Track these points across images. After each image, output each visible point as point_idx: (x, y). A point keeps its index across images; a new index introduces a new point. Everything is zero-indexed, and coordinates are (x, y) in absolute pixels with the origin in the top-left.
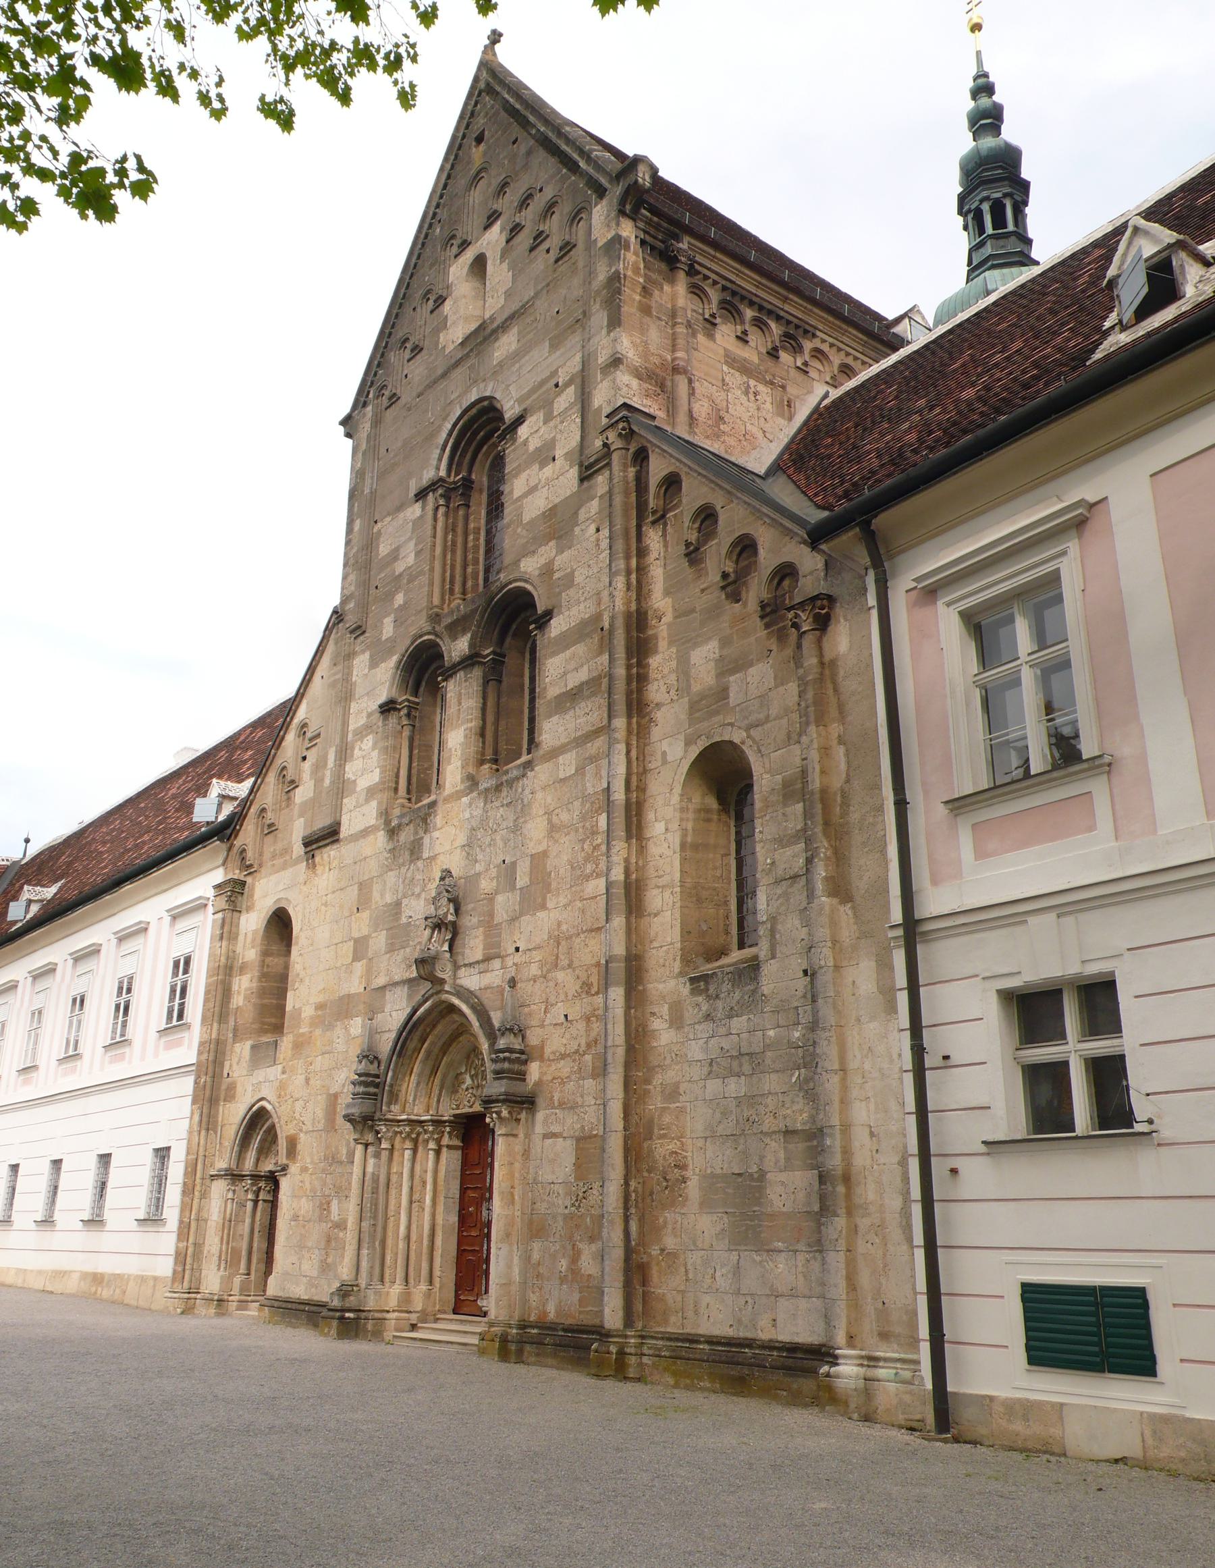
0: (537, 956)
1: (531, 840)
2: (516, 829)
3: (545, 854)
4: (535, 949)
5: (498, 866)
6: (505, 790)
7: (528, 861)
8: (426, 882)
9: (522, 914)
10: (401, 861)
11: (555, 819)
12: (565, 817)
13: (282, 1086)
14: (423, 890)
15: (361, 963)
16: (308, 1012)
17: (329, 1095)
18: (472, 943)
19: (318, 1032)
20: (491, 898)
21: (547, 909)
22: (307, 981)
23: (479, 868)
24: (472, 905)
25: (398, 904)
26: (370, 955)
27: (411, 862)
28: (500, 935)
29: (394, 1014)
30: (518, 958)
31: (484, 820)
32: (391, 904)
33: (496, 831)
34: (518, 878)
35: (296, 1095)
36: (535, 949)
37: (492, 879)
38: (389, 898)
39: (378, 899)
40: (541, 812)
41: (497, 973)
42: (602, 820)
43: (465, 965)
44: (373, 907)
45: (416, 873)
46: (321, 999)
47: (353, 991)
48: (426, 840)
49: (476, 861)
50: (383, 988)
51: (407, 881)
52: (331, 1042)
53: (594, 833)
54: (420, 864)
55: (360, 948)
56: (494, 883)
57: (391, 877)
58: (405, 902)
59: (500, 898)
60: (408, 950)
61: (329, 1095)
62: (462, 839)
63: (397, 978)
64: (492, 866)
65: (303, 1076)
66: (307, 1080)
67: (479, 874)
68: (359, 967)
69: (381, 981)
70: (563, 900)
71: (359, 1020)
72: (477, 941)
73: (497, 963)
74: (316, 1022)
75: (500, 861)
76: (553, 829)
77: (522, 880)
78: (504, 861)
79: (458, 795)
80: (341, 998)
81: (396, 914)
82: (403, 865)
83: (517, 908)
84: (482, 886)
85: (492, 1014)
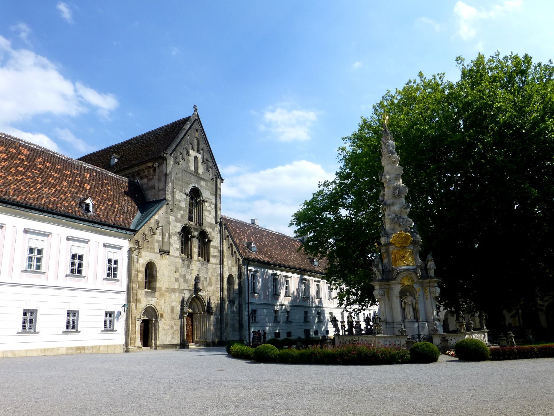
0: (210, 293)
2: (207, 272)
6: (205, 265)
12: (214, 274)
13: (157, 302)
16: (163, 288)
17: (171, 307)
19: (167, 293)
20: (203, 281)
22: (163, 282)
25: (185, 275)
31: (201, 268)
35: (162, 305)
38: (183, 273)
42: (219, 277)
46: (167, 287)
47: (176, 288)
48: (191, 266)
50: (183, 289)
52: (171, 296)
53: (218, 278)
55: (177, 280)
57: (183, 269)
59: (205, 282)
61: (171, 307)
62: (197, 269)
63: (186, 288)
65: (163, 302)
66: (165, 303)
68: (177, 284)
69: (182, 288)
70: (214, 286)
71: (178, 294)
73: (205, 292)
74: (165, 291)
76: (212, 275)
77: (208, 281)
79: (197, 261)
80: (173, 288)
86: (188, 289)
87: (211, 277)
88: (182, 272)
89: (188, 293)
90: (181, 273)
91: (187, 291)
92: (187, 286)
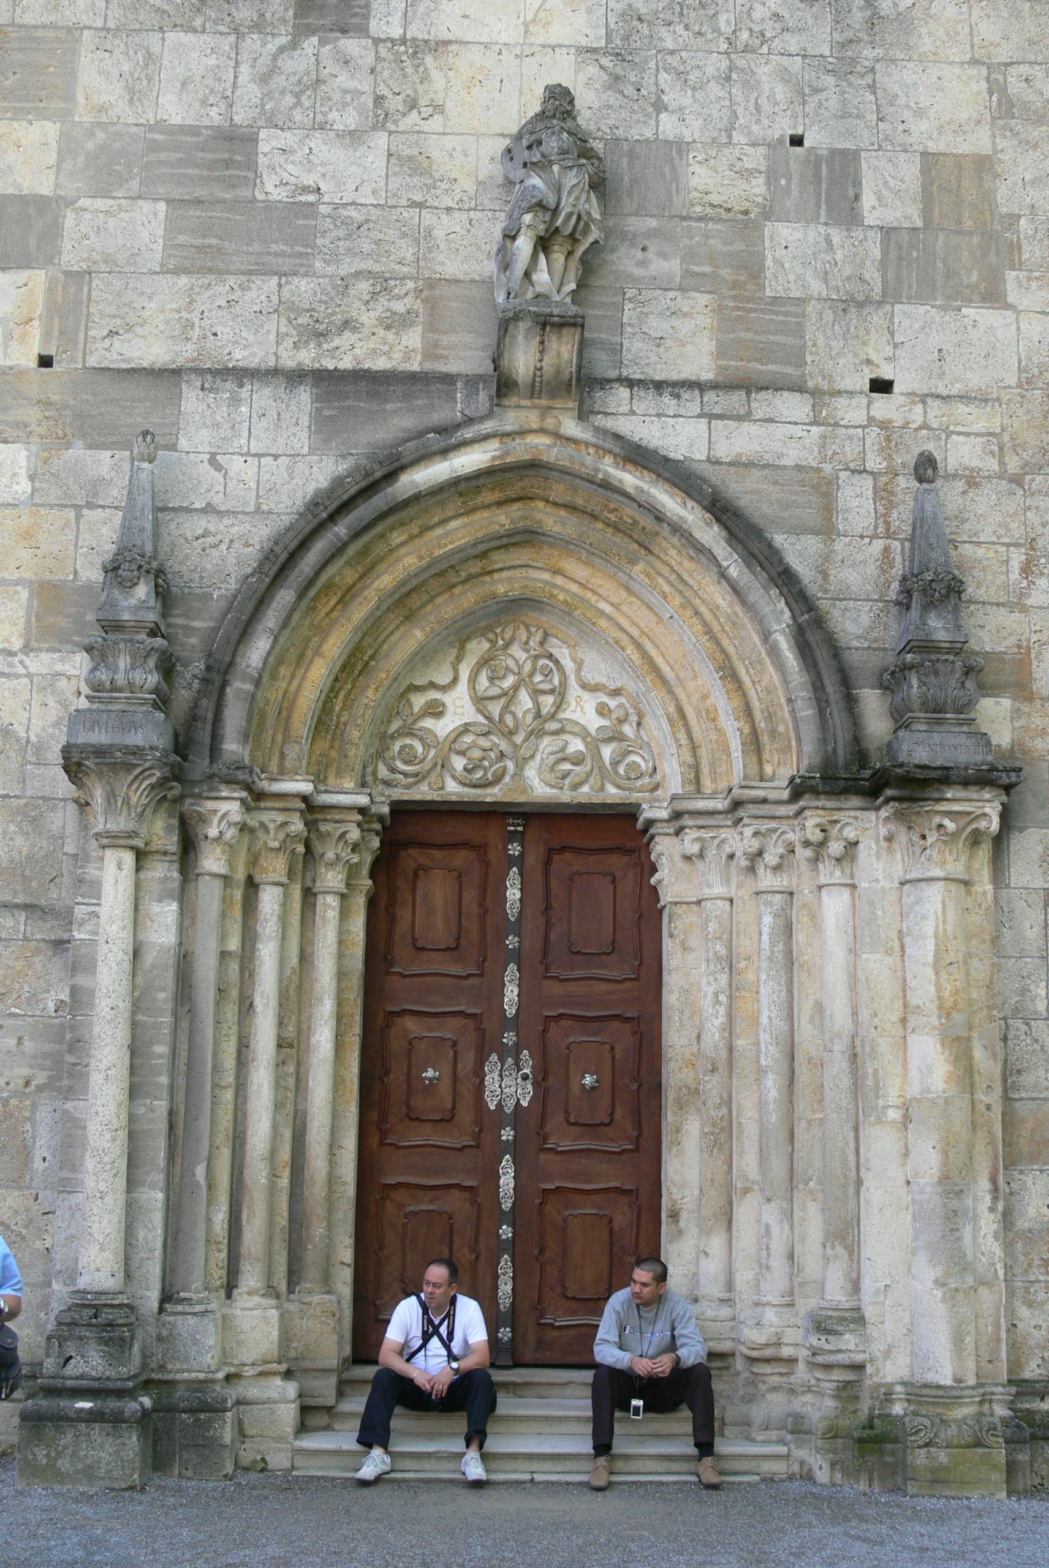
1: (920, 113)
3: (984, 165)
4: (964, 398)
5: (773, 146)
7: (910, 170)
8: (395, 104)
9: (891, 295)
10: (245, 14)
11: (1015, 86)
14: (378, 126)
15: (22, 276)
18: (656, 325)
21: (1008, 307)
23: (668, 126)
24: (652, 223)
26: (71, 257)
27: (301, 32)
28: (799, 331)
29: (235, 465)
30: (882, 406)
32: (194, 131)
33: (747, 49)
34: (868, 200)
36: (964, 398)
37: (747, 174)
39: (112, 94)
40: (957, 53)
41: (798, 431)
43: (631, 383)
44: (83, 116)
45: (331, 67)
49: (660, 107)
51: (279, 81)
54: (351, 45)
56: (758, 187)
58: (268, 141)
60: (303, 287)
63: (240, 357)
64: (737, 137)
67: (680, 147)
72: (685, 326)
75: (785, 128)
78: (797, 141)
81: (228, 164)
82: (259, 26)
83: (872, 275)
84: (694, 181)
85: (779, 539)
86: (307, 357)
87: (980, 141)
88: (133, 95)
89: (301, 440)
90: (123, 111)
91: (264, 396)
92: (287, 308)
